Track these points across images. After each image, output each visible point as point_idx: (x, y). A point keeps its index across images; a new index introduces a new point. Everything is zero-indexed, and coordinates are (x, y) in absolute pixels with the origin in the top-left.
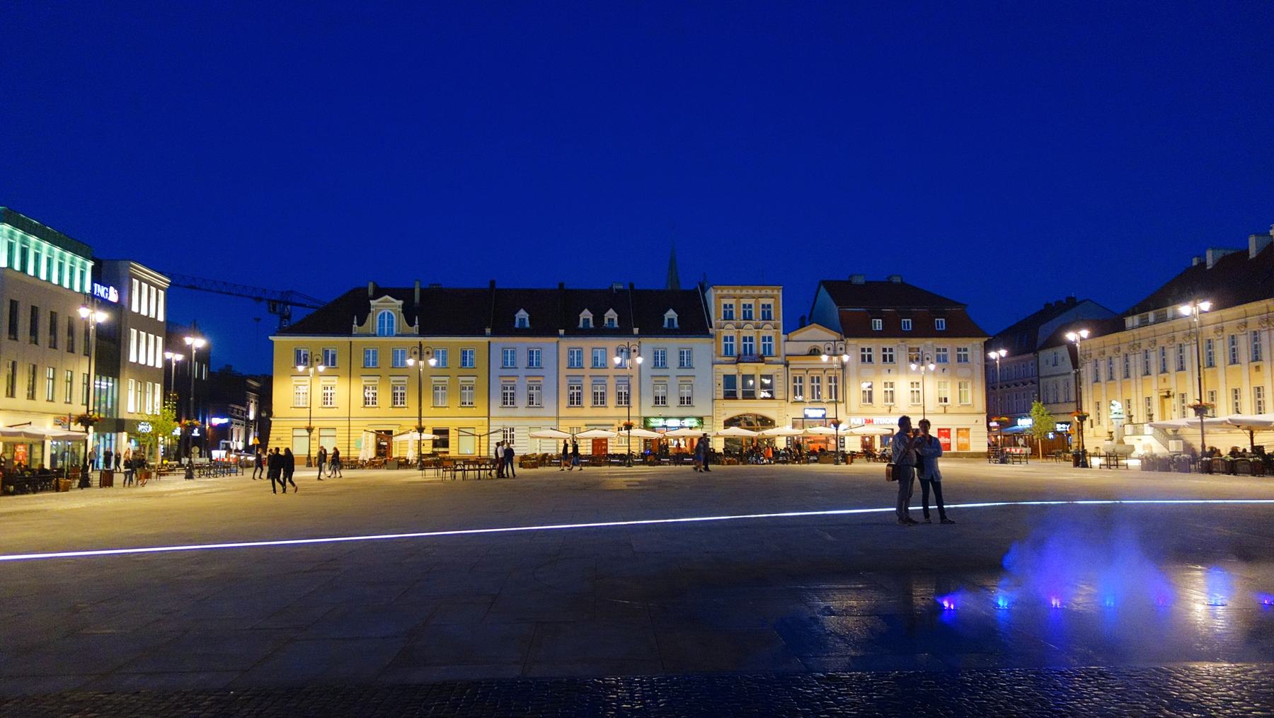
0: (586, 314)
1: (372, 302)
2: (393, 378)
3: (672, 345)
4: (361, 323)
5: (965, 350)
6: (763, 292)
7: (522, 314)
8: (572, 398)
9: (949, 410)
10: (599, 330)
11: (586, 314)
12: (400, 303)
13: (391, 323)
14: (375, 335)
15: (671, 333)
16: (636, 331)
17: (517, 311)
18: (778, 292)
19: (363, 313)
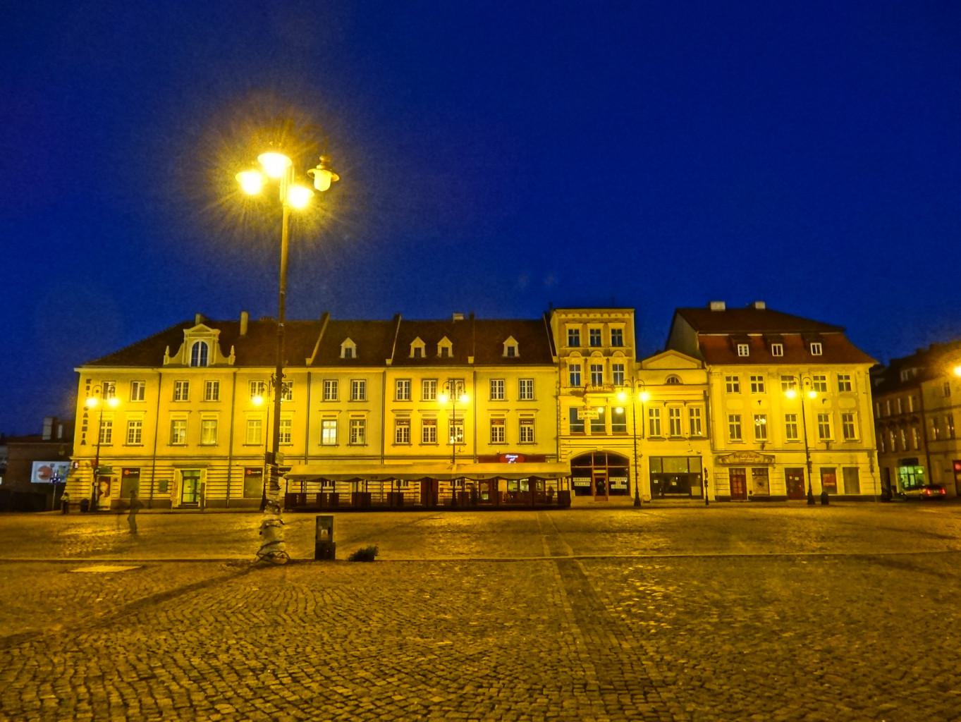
0: (418, 343)
1: (185, 331)
2: (203, 414)
3: (512, 377)
4: (172, 354)
5: (848, 377)
6: (613, 316)
7: (348, 344)
8: (399, 435)
9: (833, 447)
10: (432, 359)
11: (418, 343)
12: (217, 332)
13: (204, 354)
14: (187, 366)
15: (512, 361)
16: (471, 360)
17: (343, 340)
18: (630, 316)
19: (176, 342)
